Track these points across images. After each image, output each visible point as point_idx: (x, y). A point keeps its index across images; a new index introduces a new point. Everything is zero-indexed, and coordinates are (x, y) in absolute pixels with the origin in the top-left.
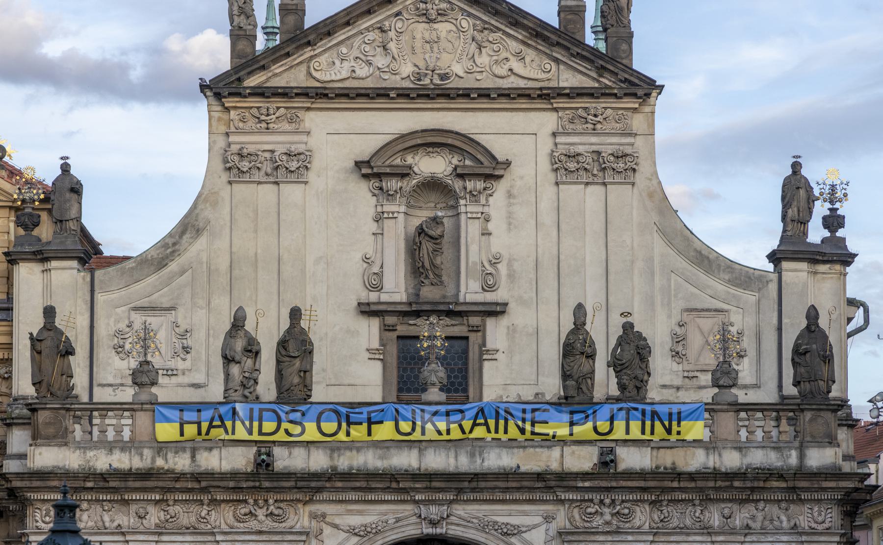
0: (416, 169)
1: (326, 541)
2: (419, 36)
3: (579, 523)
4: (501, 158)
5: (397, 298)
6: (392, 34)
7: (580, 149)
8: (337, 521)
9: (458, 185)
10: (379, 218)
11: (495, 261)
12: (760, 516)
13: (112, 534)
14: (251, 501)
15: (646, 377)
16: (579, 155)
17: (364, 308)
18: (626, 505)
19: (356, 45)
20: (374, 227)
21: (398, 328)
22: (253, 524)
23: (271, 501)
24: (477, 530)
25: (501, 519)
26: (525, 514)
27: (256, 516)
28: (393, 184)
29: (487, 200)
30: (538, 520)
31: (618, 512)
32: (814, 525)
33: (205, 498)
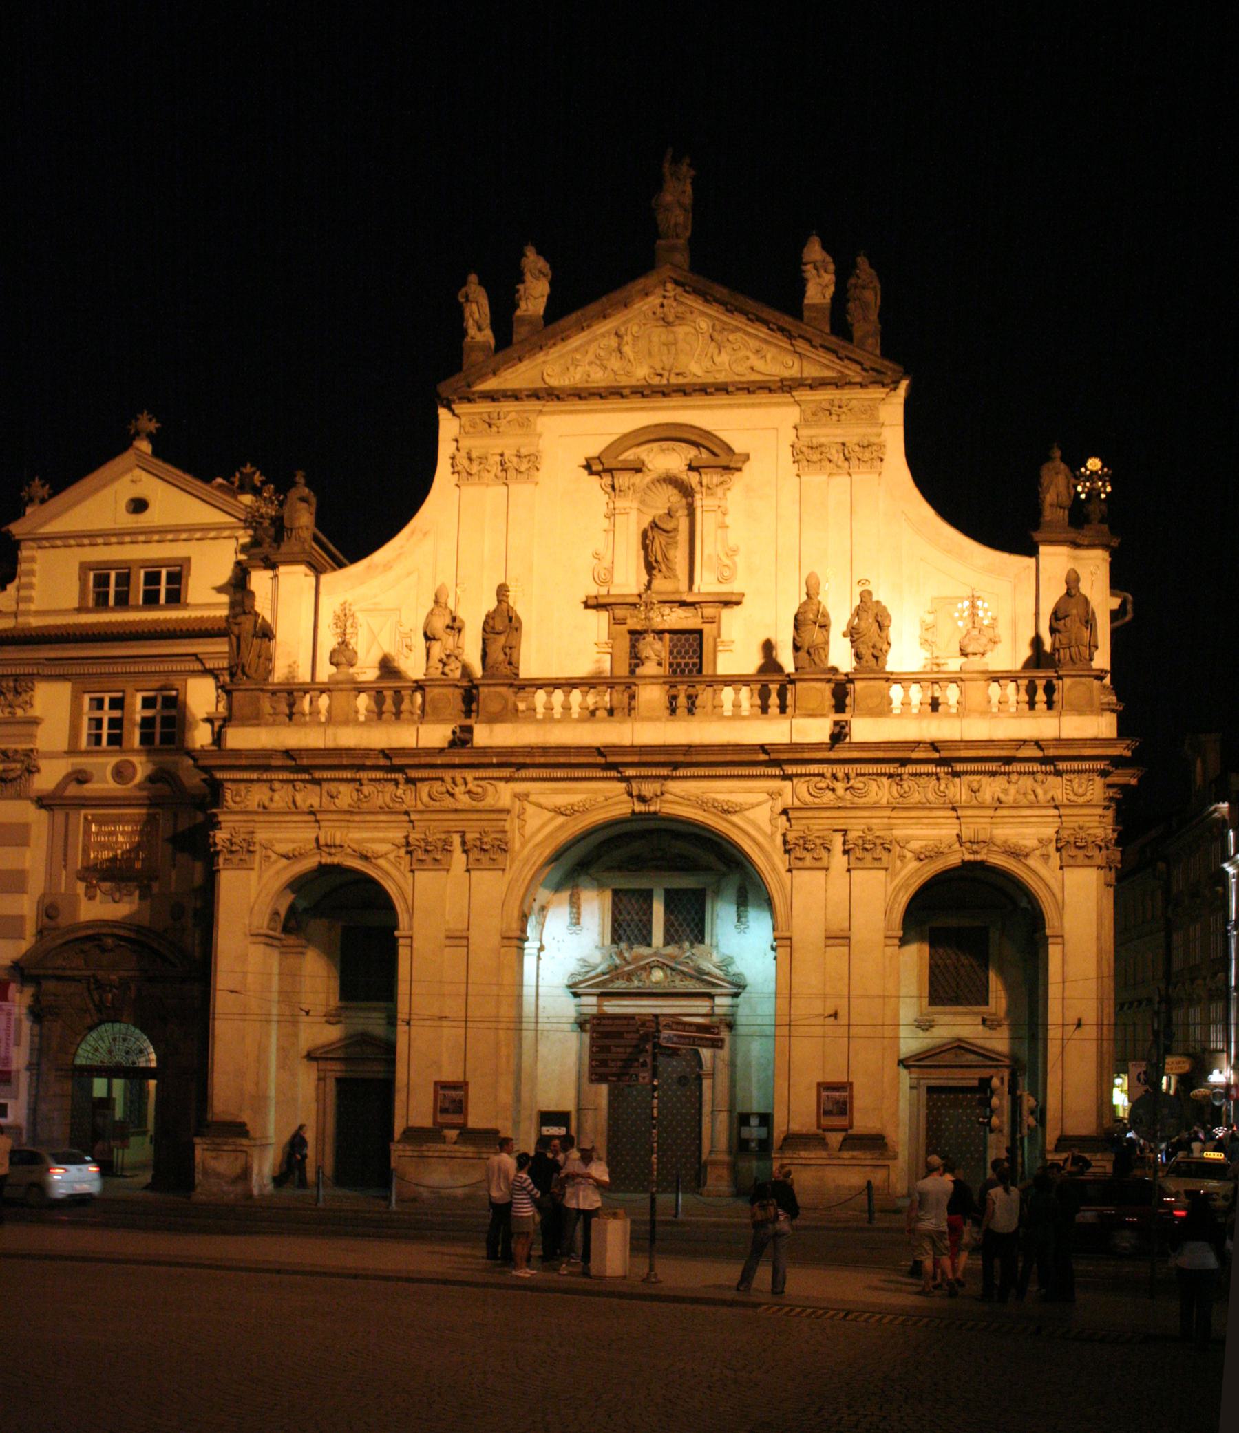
0: (650, 467)
1: (529, 821)
2: (655, 339)
3: (809, 799)
4: (738, 447)
5: (626, 591)
6: (628, 338)
7: (823, 440)
8: (542, 800)
9: (693, 478)
10: (611, 515)
11: (733, 552)
12: (1012, 789)
13: (303, 813)
14: (448, 779)
15: (885, 647)
16: (821, 446)
17: (591, 602)
18: (861, 778)
19: (592, 349)
20: (606, 523)
21: (629, 621)
22: (449, 802)
23: (469, 779)
24: (693, 807)
25: (720, 797)
26: (750, 791)
27: (452, 795)
28: (623, 480)
29: (724, 494)
30: (764, 796)
31: (852, 787)
32: (1072, 797)
33: (400, 776)
